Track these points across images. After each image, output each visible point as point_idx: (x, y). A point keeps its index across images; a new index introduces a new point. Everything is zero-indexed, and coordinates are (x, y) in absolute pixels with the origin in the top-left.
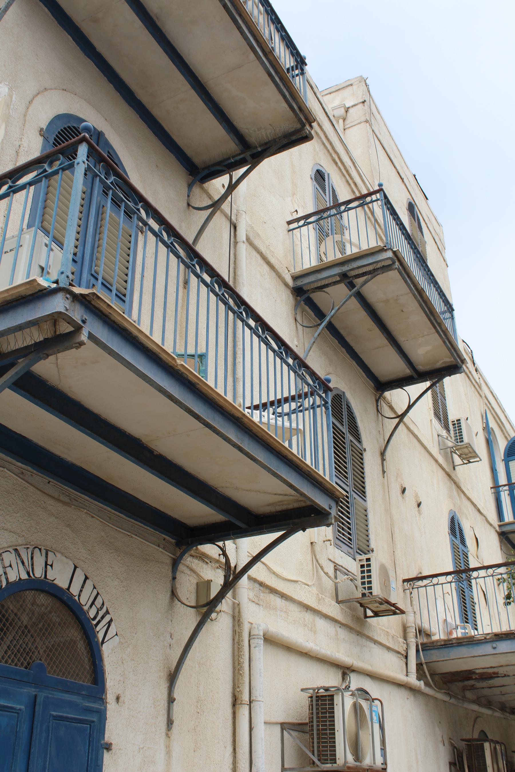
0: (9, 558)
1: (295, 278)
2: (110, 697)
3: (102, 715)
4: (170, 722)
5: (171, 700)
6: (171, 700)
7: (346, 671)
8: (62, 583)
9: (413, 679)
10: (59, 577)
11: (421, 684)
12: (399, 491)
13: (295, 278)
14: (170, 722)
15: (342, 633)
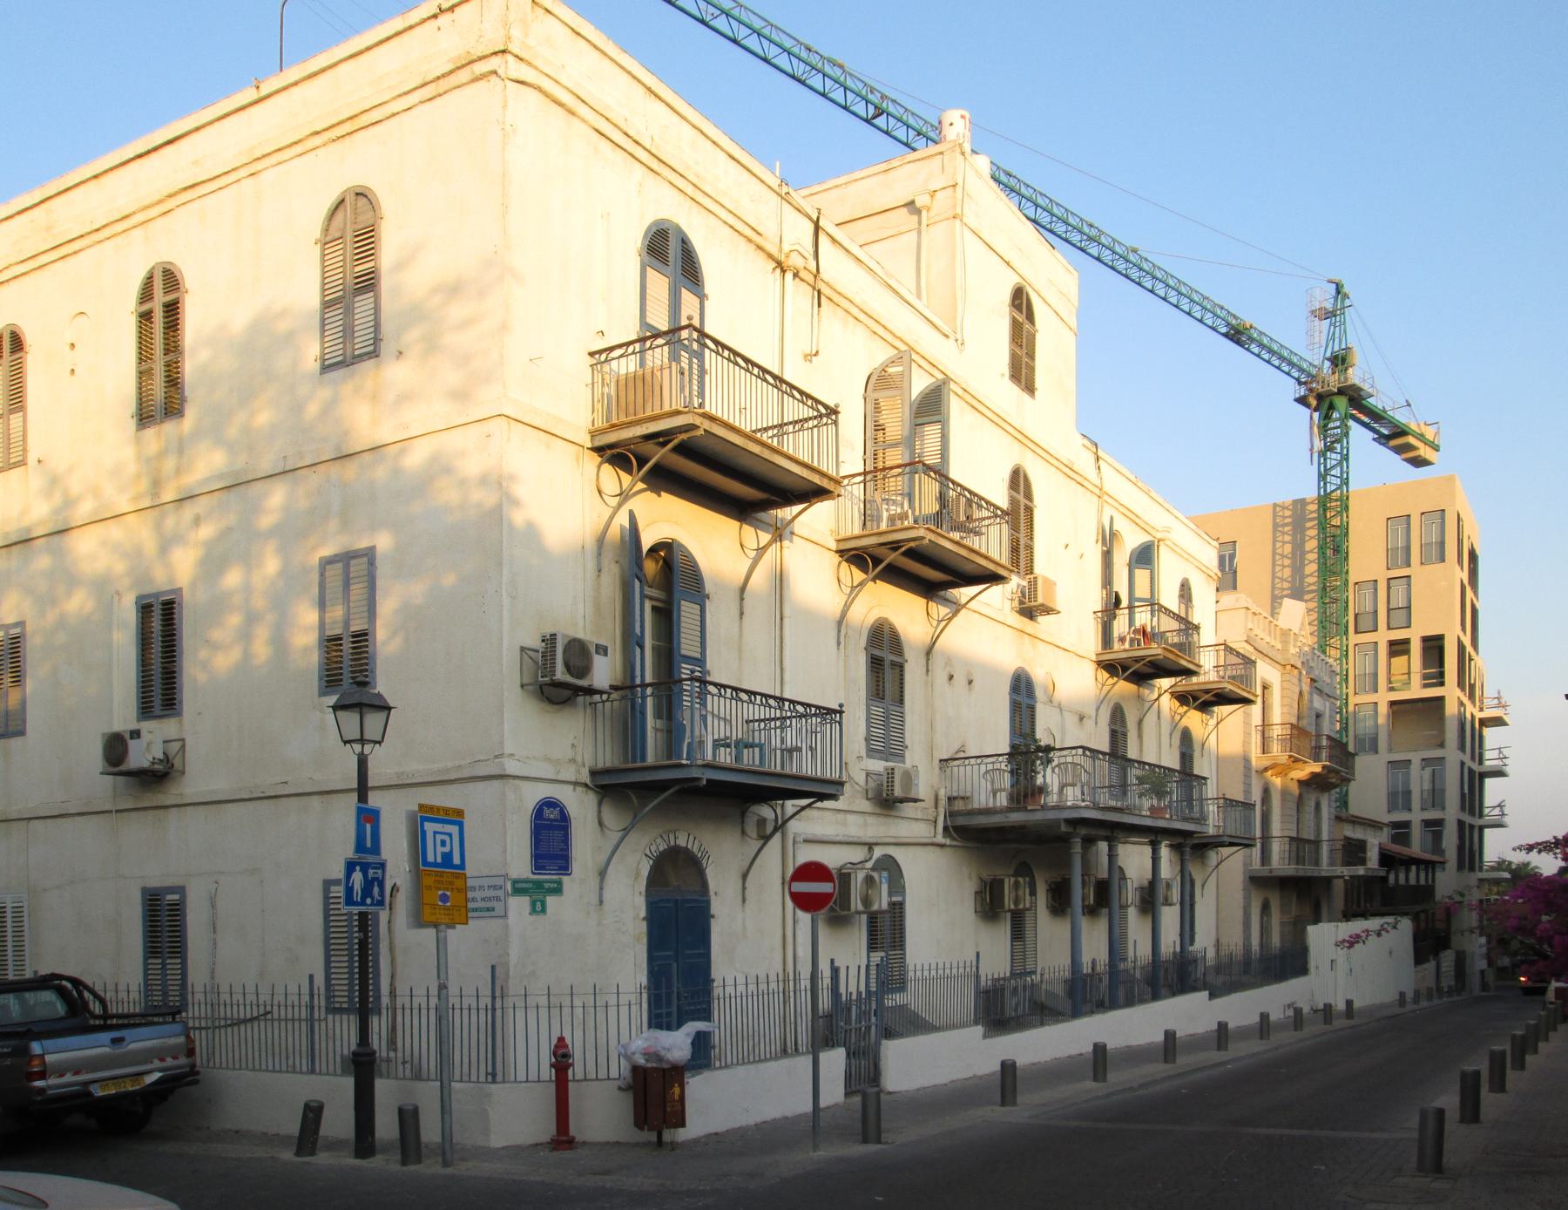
0: (659, 840)
1: (838, 541)
2: (712, 893)
3: (708, 903)
4: (744, 900)
5: (744, 888)
6: (744, 888)
7: (871, 846)
8: (683, 844)
9: (940, 839)
10: (682, 842)
11: (948, 841)
12: (946, 678)
13: (838, 541)
14: (744, 900)
15: (871, 820)
